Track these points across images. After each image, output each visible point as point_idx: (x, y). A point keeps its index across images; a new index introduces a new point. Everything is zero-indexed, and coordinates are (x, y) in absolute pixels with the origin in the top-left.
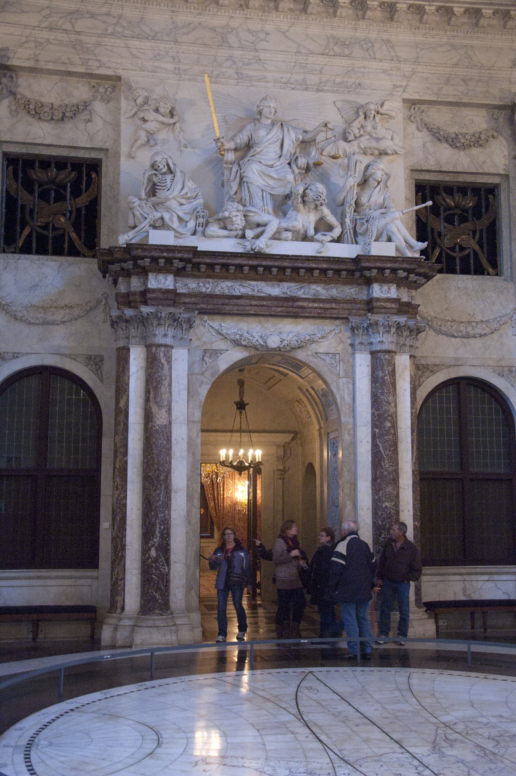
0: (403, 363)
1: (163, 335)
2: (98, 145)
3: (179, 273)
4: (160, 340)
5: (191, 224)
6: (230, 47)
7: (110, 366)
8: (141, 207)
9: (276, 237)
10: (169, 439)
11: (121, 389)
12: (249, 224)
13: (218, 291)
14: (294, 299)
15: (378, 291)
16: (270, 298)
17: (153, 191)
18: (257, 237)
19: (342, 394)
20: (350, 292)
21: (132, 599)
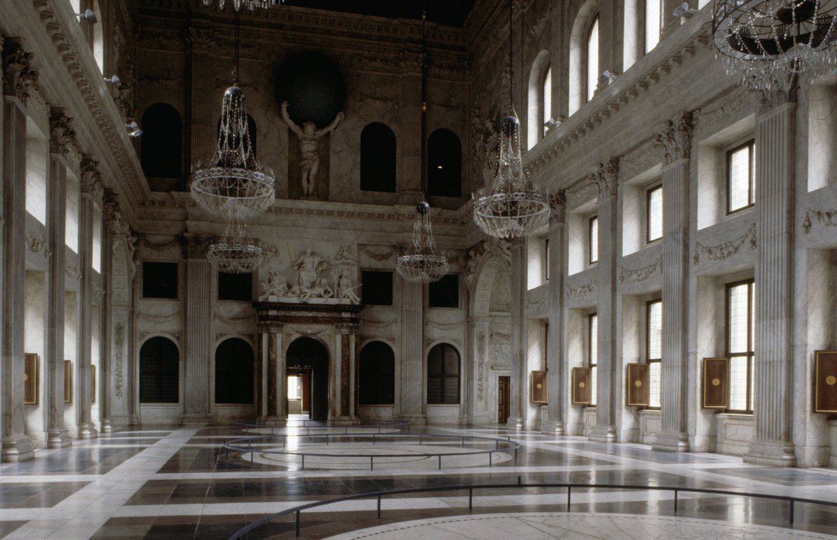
1: (273, 330)
4: (272, 332)
5: (283, 292)
6: (297, 227)
7: (256, 339)
8: (265, 286)
9: (311, 296)
10: (276, 362)
11: (260, 347)
12: (302, 293)
13: (291, 315)
14: (317, 317)
15: (344, 315)
16: (308, 317)
17: (270, 281)
18: (304, 296)
19: (331, 349)
20: (335, 314)
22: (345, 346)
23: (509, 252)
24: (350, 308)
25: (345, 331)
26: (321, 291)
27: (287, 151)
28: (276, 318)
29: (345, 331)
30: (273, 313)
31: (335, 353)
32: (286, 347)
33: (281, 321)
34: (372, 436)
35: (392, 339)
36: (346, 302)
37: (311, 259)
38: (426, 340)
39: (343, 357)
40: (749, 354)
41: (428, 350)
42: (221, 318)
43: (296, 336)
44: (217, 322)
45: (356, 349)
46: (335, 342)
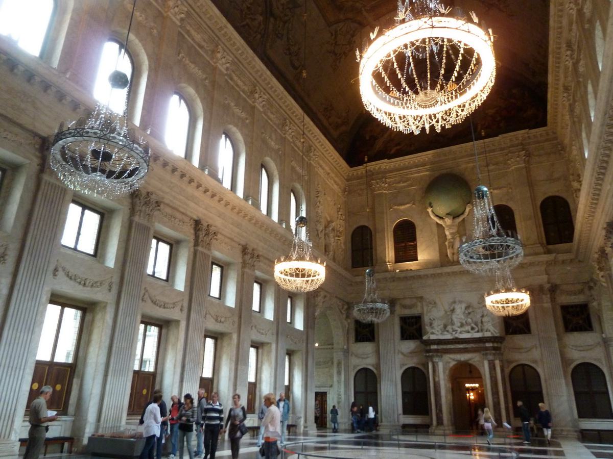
0: (497, 363)
1: (436, 359)
2: (420, 312)
5: (440, 332)
10: (439, 384)
15: (488, 345)
18: (456, 333)
20: (481, 345)
21: (435, 422)
22: (492, 368)
23: (603, 280)
24: (493, 339)
25: (491, 357)
26: (468, 328)
27: (436, 237)
28: (437, 351)
29: (491, 357)
30: (434, 347)
31: (485, 375)
32: (447, 372)
34: (434, 444)
35: (535, 362)
36: (488, 334)
37: (459, 306)
38: (565, 361)
39: (491, 377)
41: (570, 370)
42: (402, 353)
43: (453, 363)
44: (401, 356)
45: (502, 371)
46: (483, 366)
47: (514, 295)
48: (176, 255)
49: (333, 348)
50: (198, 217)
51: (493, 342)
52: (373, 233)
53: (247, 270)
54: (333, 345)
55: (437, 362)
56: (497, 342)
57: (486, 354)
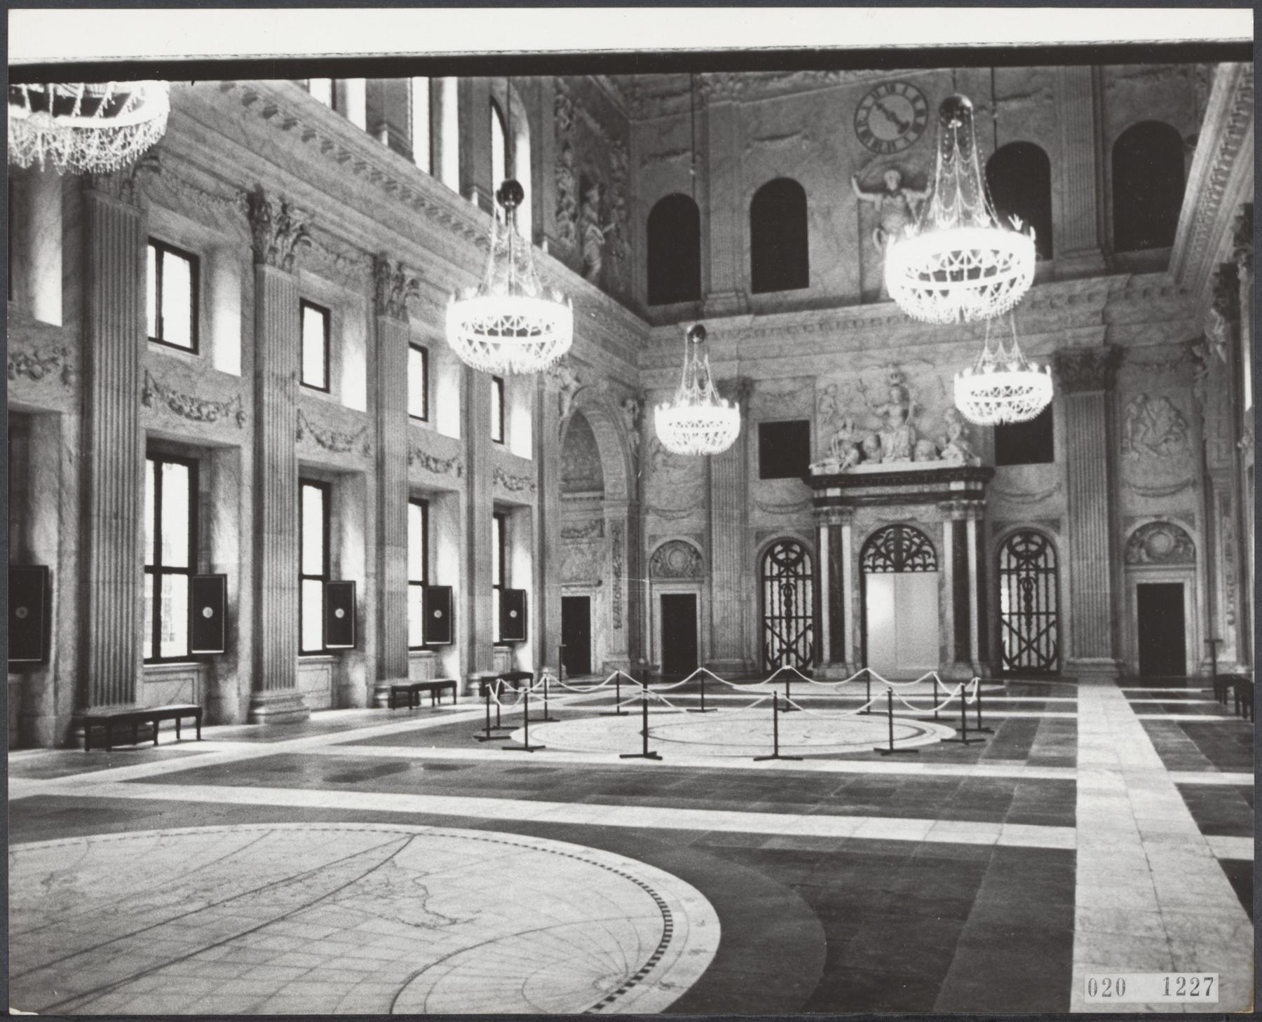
3: (842, 487)
20: (941, 488)
28: (841, 500)
29: (956, 514)
30: (834, 492)
33: (848, 505)
40: (158, 570)
42: (763, 507)
47: (1013, 377)
48: (210, 288)
49: (602, 498)
50: (258, 186)
51: (967, 480)
52: (702, 217)
53: (388, 320)
54: (602, 489)
55: (839, 527)
56: (976, 480)
57: (950, 508)
